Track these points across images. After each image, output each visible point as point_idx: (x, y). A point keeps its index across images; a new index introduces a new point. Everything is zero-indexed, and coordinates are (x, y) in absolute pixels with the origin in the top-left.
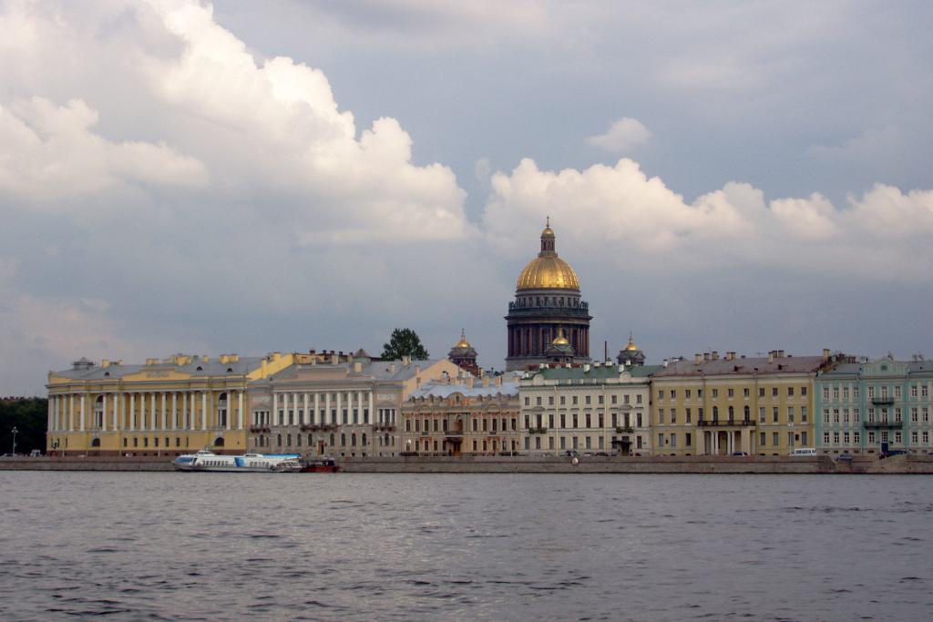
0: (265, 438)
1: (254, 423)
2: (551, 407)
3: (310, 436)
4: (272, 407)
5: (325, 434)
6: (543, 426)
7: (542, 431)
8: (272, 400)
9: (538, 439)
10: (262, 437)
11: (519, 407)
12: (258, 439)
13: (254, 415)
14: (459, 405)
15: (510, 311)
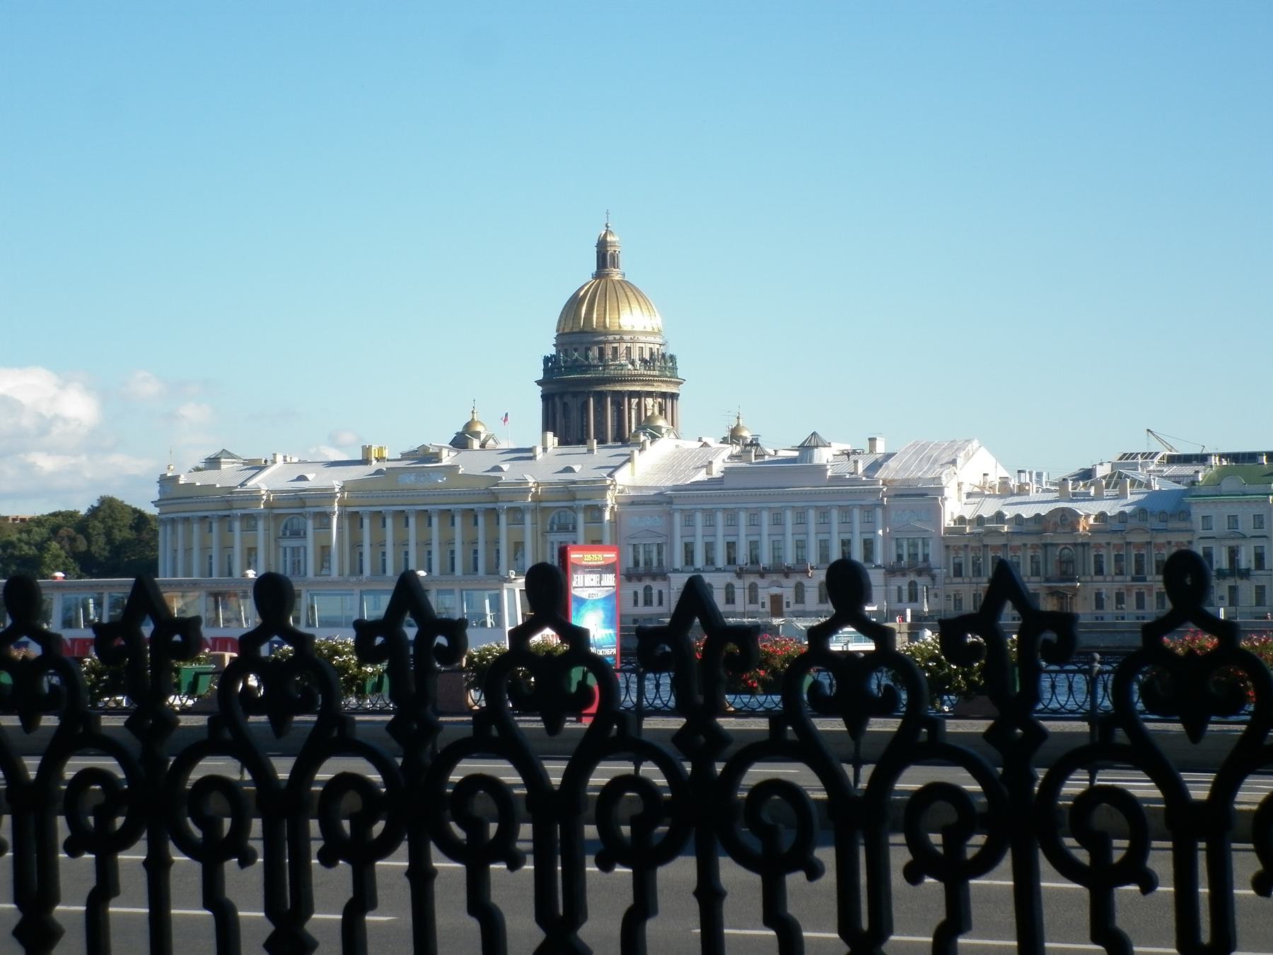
0: (655, 592)
1: (631, 564)
2: (1258, 532)
3: (753, 589)
4: (670, 535)
5: (785, 581)
6: (1243, 565)
7: (1246, 574)
8: (671, 524)
9: (1233, 590)
10: (648, 589)
11: (1191, 531)
12: (905, 588)
13: (631, 549)
14: (1068, 530)
15: (546, 371)
